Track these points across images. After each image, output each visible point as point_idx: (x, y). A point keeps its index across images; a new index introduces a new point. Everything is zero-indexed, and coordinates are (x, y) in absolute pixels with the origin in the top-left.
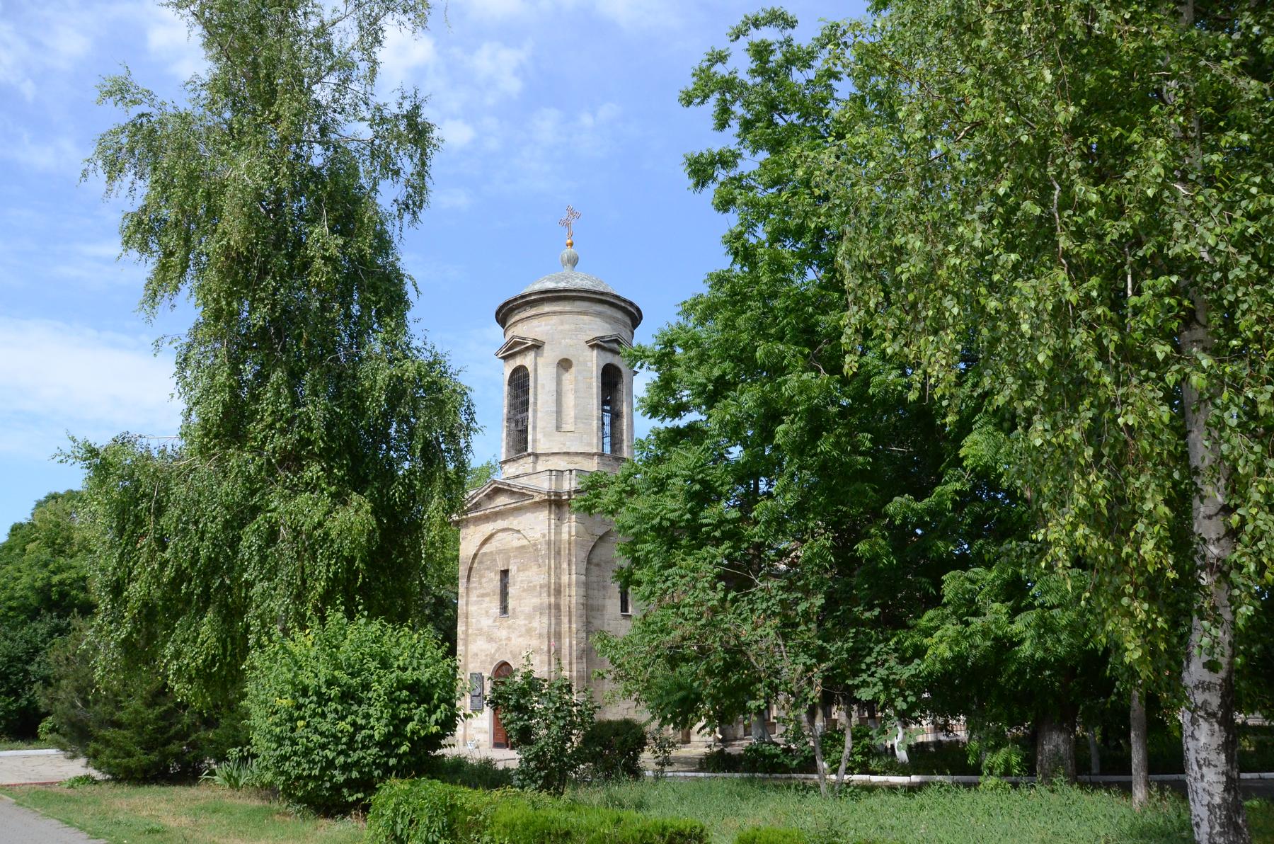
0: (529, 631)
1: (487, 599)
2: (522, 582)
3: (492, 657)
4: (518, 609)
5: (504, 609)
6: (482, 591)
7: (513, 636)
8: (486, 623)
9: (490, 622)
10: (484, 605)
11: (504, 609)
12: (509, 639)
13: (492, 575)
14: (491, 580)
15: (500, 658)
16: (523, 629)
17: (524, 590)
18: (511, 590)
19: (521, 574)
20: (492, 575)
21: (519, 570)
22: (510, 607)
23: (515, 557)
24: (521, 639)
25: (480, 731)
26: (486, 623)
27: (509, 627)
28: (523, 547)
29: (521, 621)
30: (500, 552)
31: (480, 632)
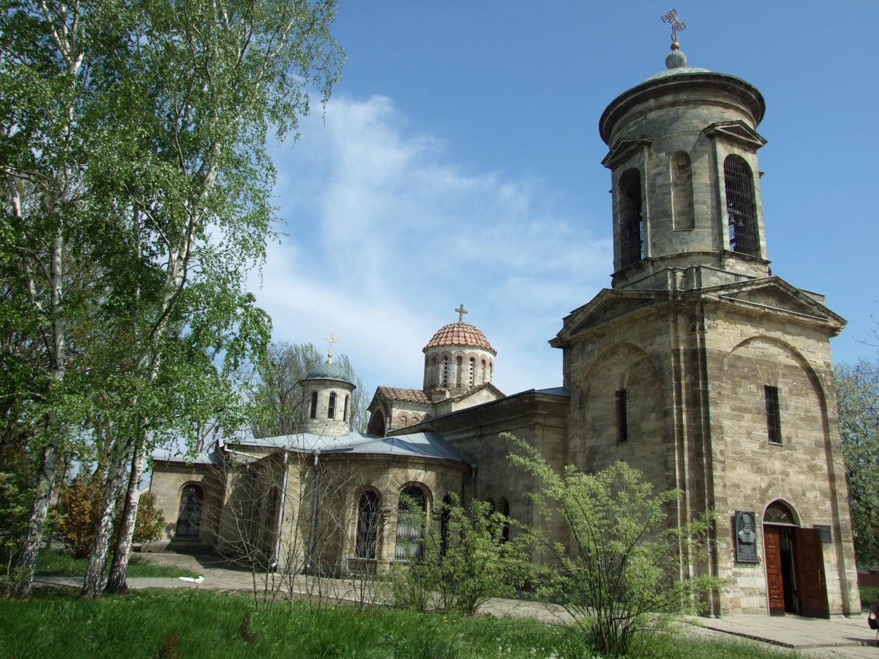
0: (812, 469)
1: (748, 416)
2: (796, 408)
3: (764, 492)
4: (793, 440)
5: (775, 435)
6: (738, 403)
7: (791, 471)
8: (749, 447)
9: (755, 446)
10: (744, 423)
11: (775, 435)
12: (786, 474)
13: (753, 386)
14: (752, 394)
15: (775, 496)
16: (805, 465)
17: (803, 419)
18: (783, 415)
19: (795, 398)
20: (753, 386)
21: (791, 393)
22: (785, 431)
23: (784, 376)
24: (802, 477)
25: (750, 592)
26: (749, 447)
27: (784, 458)
28: (796, 368)
29: (799, 455)
30: (760, 361)
31: (741, 457)
